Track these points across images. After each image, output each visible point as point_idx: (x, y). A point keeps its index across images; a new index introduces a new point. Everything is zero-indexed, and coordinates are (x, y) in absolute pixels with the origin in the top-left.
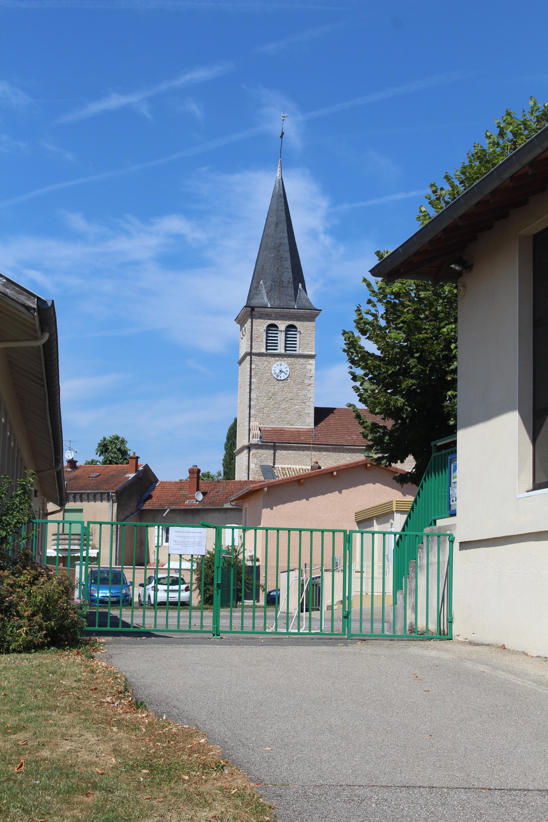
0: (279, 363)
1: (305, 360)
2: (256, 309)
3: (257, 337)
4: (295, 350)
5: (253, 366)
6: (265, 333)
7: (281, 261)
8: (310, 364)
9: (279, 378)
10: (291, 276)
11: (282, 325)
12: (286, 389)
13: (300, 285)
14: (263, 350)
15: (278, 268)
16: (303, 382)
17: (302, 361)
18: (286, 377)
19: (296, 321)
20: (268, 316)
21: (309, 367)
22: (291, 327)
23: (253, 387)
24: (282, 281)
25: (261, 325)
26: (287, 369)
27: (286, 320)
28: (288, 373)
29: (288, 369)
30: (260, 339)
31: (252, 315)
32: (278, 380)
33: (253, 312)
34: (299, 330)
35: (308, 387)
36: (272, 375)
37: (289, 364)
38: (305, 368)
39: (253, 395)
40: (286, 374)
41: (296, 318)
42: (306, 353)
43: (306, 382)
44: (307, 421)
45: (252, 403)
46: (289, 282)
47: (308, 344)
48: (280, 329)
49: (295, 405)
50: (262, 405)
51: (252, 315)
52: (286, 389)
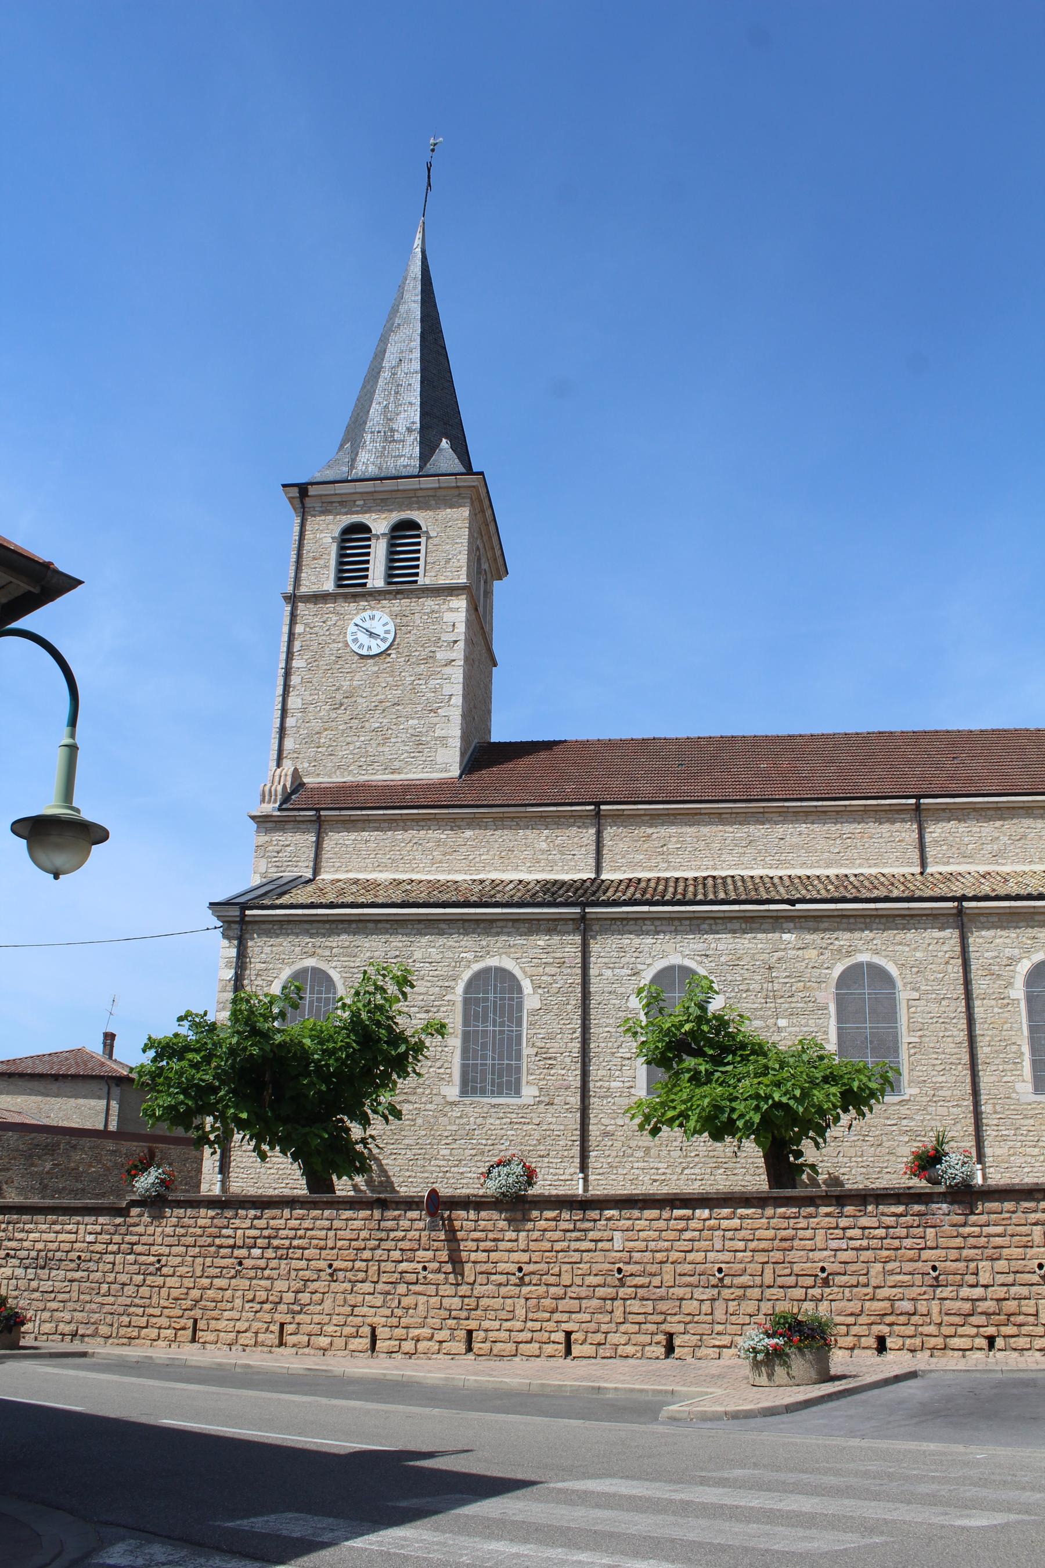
0: (366, 614)
1: (439, 600)
2: (312, 491)
3: (315, 559)
4: (416, 582)
5: (299, 629)
6: (334, 549)
7: (397, 393)
8: (451, 610)
9: (364, 652)
10: (417, 419)
11: (380, 524)
12: (385, 679)
13: (444, 440)
14: (329, 586)
15: (386, 407)
16: (432, 656)
17: (429, 603)
18: (384, 646)
19: (419, 509)
20: (344, 504)
21: (449, 617)
22: (405, 528)
23: (295, 680)
24: (392, 430)
25: (325, 532)
26: (386, 628)
27: (391, 511)
28: (391, 637)
29: (391, 627)
30: (322, 562)
31: (303, 507)
32: (362, 657)
33: (308, 501)
34: (424, 529)
35: (447, 670)
36: (347, 645)
37: (394, 616)
38: (438, 621)
39: (294, 702)
40: (384, 640)
41: (418, 503)
42: (442, 581)
43: (439, 655)
44: (439, 760)
45: (290, 722)
46: (409, 430)
47: (448, 561)
48: (374, 532)
49: (408, 718)
50: (316, 725)
51: (303, 507)
52: (385, 679)
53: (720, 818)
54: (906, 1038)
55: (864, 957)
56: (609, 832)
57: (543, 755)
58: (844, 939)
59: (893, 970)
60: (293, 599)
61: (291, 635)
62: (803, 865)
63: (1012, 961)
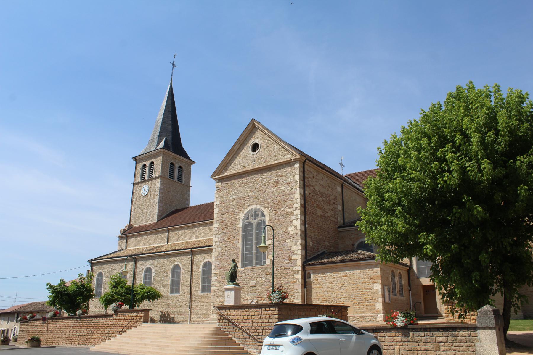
2: (137, 158)
5: (134, 191)
11: (148, 163)
17: (154, 181)
22: (152, 163)
39: (133, 208)
45: (132, 213)
53: (189, 228)
54: (181, 281)
55: (176, 263)
56: (171, 233)
57: (183, 212)
58: (174, 259)
59: (181, 266)
60: (134, 184)
61: (133, 192)
62: (202, 237)
63: (201, 262)
